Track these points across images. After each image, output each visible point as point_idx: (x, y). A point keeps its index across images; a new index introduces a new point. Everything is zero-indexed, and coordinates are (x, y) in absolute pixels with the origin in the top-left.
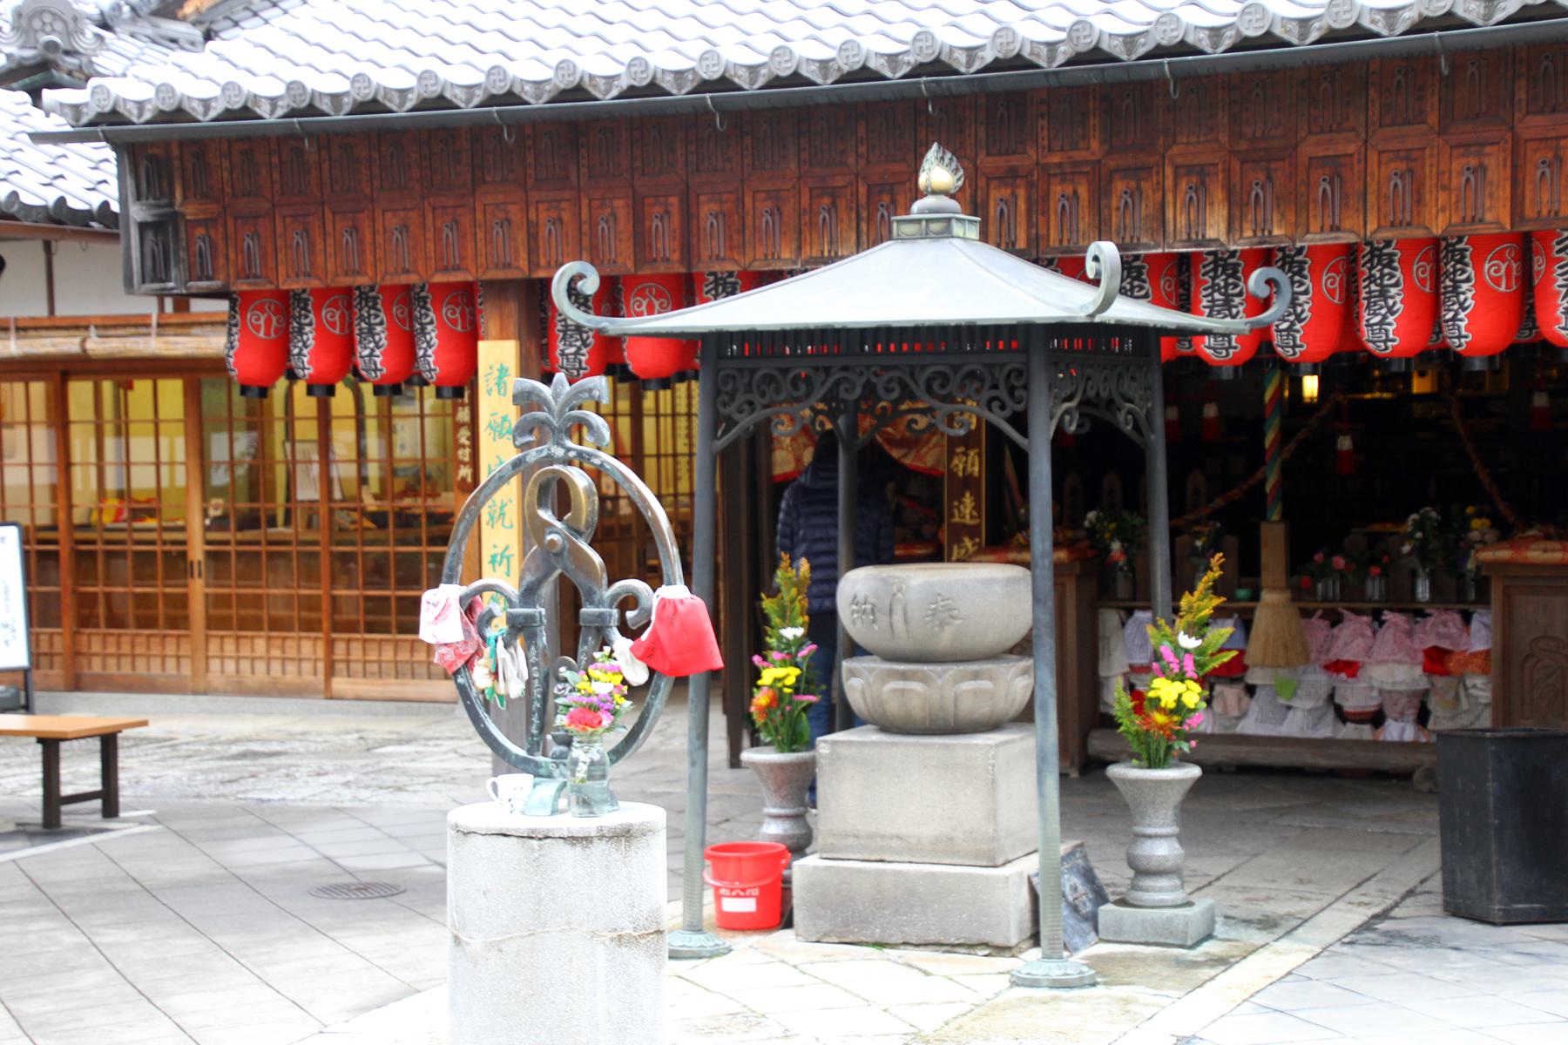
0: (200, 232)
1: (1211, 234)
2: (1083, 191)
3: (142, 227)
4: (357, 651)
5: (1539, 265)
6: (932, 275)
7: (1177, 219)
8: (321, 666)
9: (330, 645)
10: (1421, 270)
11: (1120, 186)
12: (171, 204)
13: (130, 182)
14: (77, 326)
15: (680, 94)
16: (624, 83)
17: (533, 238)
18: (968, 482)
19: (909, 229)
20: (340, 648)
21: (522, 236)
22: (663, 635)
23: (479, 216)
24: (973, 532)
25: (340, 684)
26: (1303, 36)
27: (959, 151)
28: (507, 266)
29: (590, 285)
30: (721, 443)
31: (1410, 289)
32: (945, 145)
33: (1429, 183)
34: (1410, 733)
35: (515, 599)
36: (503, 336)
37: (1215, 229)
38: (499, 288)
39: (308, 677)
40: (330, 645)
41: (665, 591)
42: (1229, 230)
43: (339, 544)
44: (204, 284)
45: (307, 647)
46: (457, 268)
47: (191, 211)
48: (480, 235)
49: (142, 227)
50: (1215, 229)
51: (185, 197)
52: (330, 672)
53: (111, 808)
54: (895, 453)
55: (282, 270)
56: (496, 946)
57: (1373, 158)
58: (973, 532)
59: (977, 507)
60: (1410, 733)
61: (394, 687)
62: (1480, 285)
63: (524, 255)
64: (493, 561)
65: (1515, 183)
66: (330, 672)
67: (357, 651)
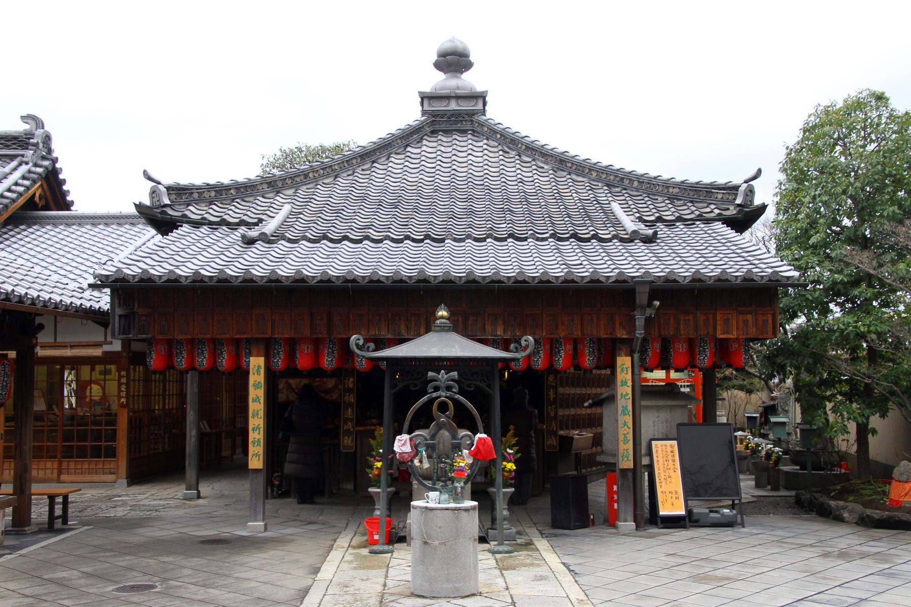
0: (144, 318)
1: (499, 333)
2: (460, 319)
3: (120, 316)
4: (72, 465)
5: (580, 346)
6: (442, 344)
7: (489, 328)
8: (55, 471)
9: (60, 463)
10: (548, 347)
11: (471, 318)
12: (133, 309)
13: (117, 301)
14: (64, 346)
15: (338, 283)
16: (319, 279)
17: (273, 323)
18: (350, 405)
19: (437, 328)
20: (65, 465)
21: (270, 324)
22: (481, 447)
23: (254, 318)
24: (351, 420)
25: (63, 477)
26: (533, 281)
27: (449, 308)
28: (263, 333)
29: (361, 342)
30: (393, 391)
31: (545, 352)
32: (445, 305)
33: (617, 325)
34: (483, 480)
35: (428, 437)
36: (258, 356)
37: (499, 332)
38: (257, 341)
39: (49, 475)
40: (60, 463)
41: (479, 435)
42: (504, 332)
43: (81, 426)
44: (144, 336)
45: (49, 465)
46: (244, 333)
47: (141, 311)
48: (254, 323)
49: (120, 316)
50: (499, 332)
51: (139, 306)
52: (60, 473)
53: (65, 522)
54: (323, 395)
55: (176, 332)
56: (444, 544)
57: (544, 316)
58: (351, 420)
59: (353, 412)
60: (483, 480)
61: (88, 478)
62: (566, 351)
63: (270, 330)
64: (253, 429)
65: (582, 325)
66: (60, 473)
67: (72, 465)
